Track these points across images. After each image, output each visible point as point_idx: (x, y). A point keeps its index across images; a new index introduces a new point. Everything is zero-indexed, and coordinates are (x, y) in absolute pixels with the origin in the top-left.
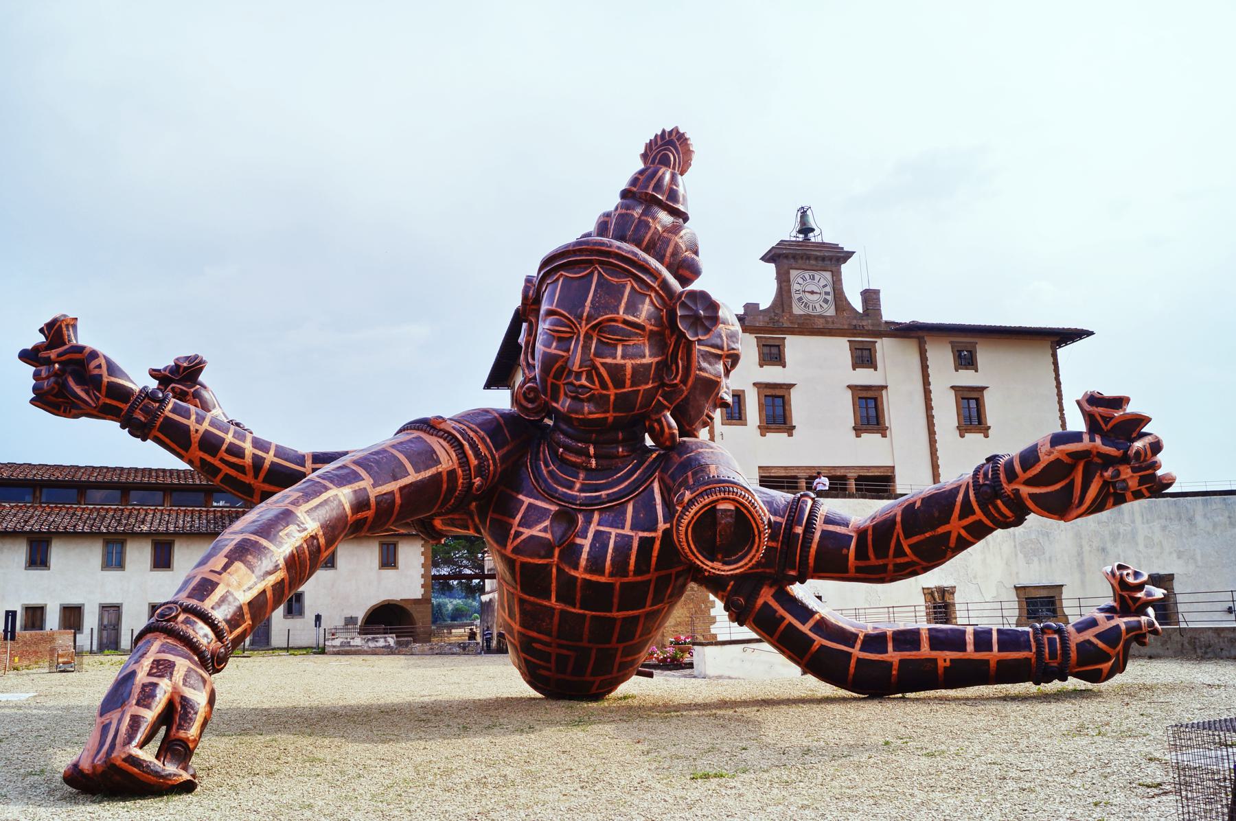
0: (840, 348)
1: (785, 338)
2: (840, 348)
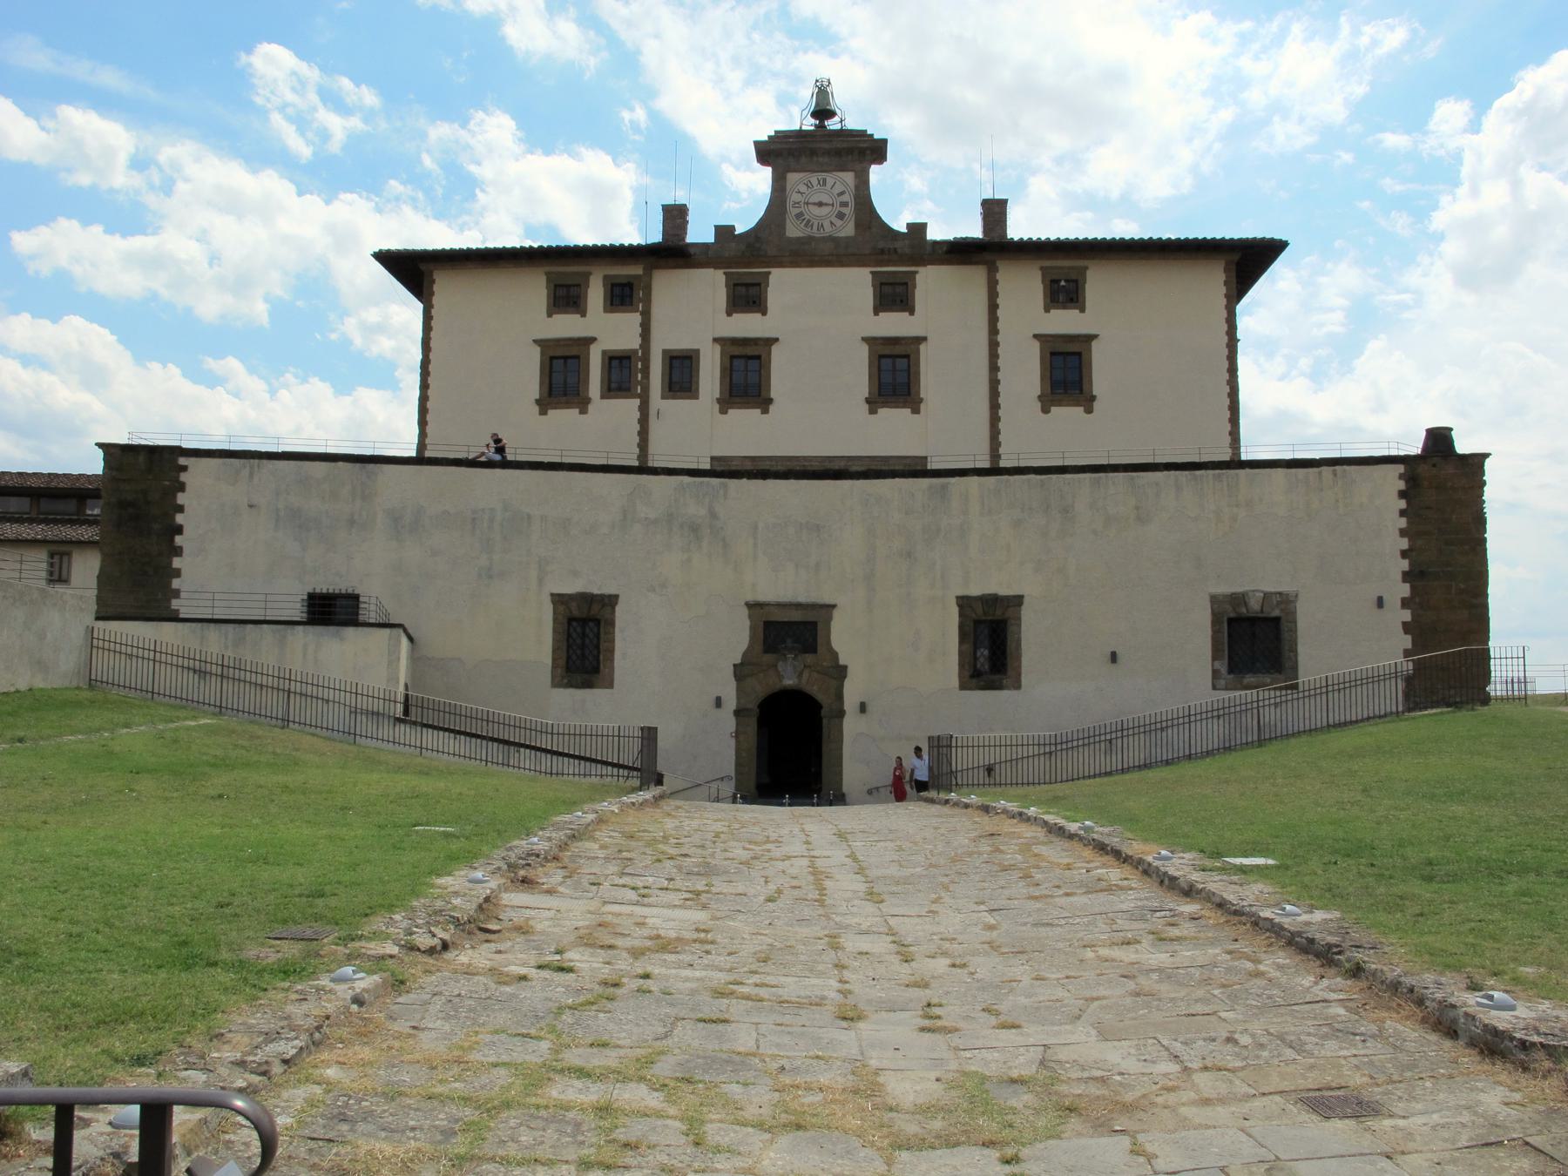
0: (857, 283)
1: (770, 273)
2: (857, 283)
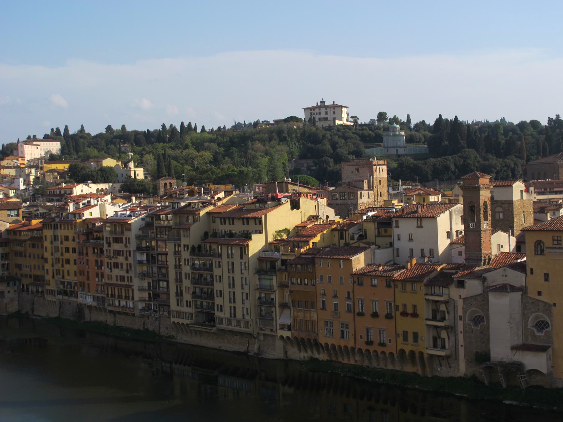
0: (324, 109)
2: (324, 109)
